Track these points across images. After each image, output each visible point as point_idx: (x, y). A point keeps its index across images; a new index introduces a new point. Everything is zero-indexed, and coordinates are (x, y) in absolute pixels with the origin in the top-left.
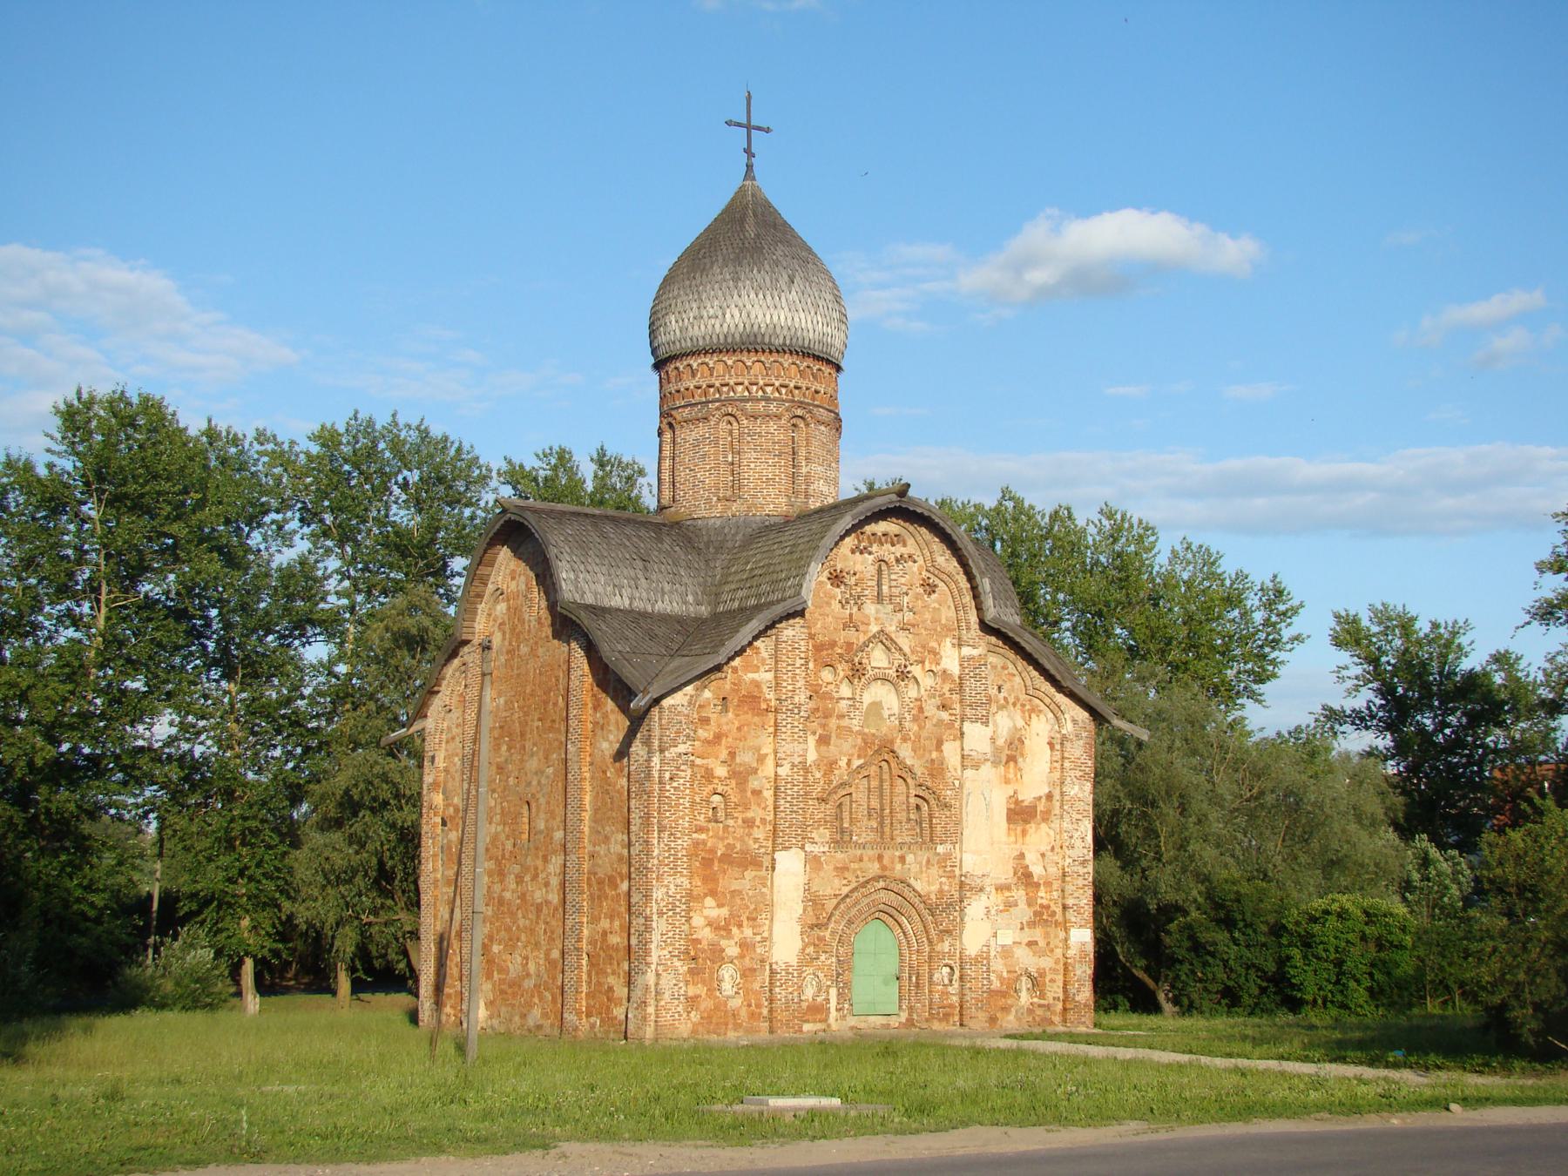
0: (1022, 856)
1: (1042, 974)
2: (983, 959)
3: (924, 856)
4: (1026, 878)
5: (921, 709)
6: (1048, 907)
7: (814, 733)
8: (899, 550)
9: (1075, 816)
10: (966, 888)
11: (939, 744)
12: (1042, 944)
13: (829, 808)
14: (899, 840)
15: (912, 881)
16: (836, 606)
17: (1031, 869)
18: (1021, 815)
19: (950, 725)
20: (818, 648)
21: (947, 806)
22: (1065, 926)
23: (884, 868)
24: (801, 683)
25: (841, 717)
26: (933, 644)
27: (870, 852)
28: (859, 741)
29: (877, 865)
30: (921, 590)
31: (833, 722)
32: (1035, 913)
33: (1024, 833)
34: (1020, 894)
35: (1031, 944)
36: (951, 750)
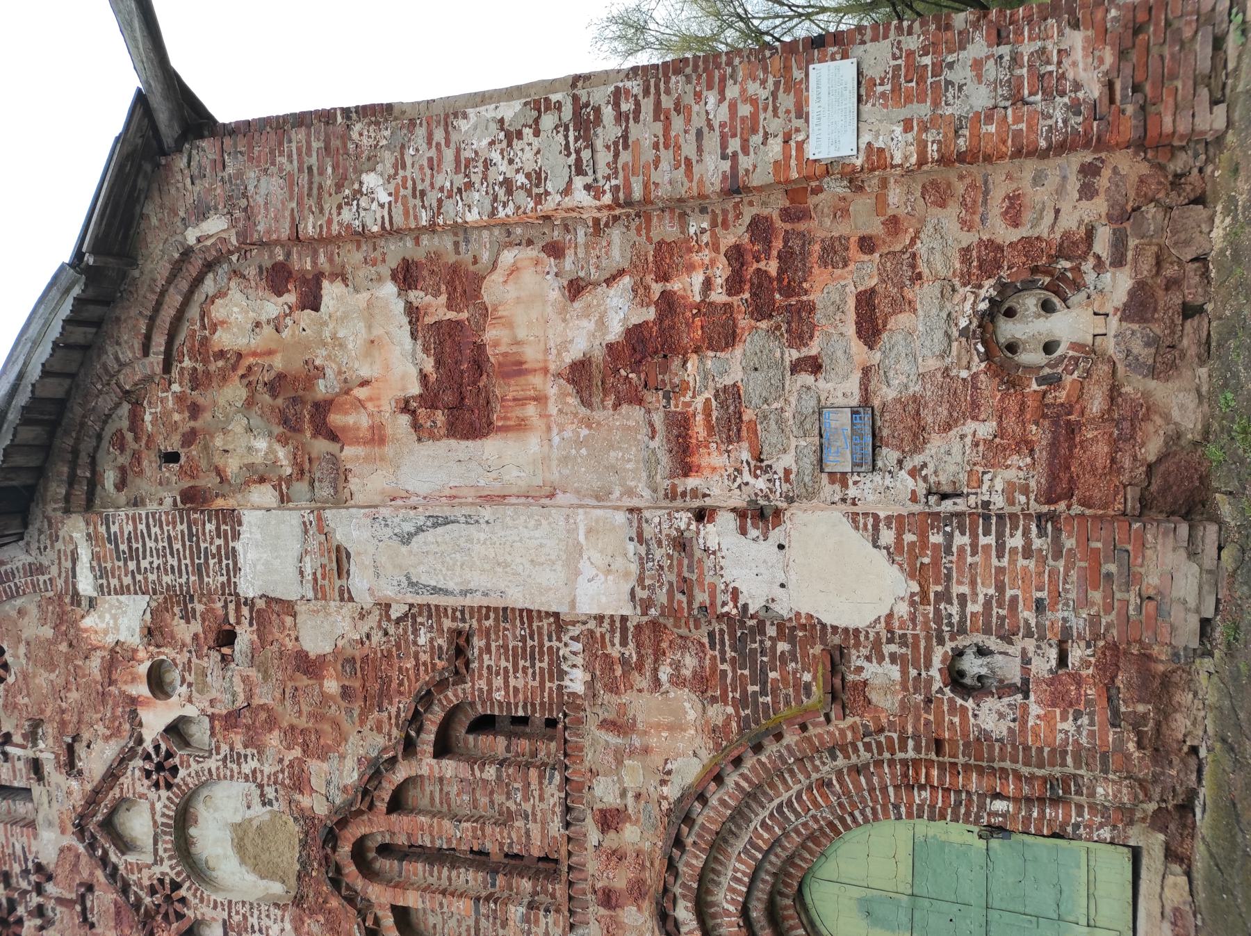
0: (579, 373)
1: (984, 260)
2: (924, 538)
3: (596, 743)
4: (640, 360)
5: (231, 720)
6: (736, 255)
9: (444, 180)
10: (681, 620)
11: (308, 666)
12: (864, 272)
15: (672, 792)
17: (615, 332)
18: (463, 392)
21: (460, 647)
22: (801, 187)
23: (637, 891)
26: (95, 665)
32: (761, 311)
33: (516, 368)
34: (701, 376)
35: (870, 328)
36: (320, 632)
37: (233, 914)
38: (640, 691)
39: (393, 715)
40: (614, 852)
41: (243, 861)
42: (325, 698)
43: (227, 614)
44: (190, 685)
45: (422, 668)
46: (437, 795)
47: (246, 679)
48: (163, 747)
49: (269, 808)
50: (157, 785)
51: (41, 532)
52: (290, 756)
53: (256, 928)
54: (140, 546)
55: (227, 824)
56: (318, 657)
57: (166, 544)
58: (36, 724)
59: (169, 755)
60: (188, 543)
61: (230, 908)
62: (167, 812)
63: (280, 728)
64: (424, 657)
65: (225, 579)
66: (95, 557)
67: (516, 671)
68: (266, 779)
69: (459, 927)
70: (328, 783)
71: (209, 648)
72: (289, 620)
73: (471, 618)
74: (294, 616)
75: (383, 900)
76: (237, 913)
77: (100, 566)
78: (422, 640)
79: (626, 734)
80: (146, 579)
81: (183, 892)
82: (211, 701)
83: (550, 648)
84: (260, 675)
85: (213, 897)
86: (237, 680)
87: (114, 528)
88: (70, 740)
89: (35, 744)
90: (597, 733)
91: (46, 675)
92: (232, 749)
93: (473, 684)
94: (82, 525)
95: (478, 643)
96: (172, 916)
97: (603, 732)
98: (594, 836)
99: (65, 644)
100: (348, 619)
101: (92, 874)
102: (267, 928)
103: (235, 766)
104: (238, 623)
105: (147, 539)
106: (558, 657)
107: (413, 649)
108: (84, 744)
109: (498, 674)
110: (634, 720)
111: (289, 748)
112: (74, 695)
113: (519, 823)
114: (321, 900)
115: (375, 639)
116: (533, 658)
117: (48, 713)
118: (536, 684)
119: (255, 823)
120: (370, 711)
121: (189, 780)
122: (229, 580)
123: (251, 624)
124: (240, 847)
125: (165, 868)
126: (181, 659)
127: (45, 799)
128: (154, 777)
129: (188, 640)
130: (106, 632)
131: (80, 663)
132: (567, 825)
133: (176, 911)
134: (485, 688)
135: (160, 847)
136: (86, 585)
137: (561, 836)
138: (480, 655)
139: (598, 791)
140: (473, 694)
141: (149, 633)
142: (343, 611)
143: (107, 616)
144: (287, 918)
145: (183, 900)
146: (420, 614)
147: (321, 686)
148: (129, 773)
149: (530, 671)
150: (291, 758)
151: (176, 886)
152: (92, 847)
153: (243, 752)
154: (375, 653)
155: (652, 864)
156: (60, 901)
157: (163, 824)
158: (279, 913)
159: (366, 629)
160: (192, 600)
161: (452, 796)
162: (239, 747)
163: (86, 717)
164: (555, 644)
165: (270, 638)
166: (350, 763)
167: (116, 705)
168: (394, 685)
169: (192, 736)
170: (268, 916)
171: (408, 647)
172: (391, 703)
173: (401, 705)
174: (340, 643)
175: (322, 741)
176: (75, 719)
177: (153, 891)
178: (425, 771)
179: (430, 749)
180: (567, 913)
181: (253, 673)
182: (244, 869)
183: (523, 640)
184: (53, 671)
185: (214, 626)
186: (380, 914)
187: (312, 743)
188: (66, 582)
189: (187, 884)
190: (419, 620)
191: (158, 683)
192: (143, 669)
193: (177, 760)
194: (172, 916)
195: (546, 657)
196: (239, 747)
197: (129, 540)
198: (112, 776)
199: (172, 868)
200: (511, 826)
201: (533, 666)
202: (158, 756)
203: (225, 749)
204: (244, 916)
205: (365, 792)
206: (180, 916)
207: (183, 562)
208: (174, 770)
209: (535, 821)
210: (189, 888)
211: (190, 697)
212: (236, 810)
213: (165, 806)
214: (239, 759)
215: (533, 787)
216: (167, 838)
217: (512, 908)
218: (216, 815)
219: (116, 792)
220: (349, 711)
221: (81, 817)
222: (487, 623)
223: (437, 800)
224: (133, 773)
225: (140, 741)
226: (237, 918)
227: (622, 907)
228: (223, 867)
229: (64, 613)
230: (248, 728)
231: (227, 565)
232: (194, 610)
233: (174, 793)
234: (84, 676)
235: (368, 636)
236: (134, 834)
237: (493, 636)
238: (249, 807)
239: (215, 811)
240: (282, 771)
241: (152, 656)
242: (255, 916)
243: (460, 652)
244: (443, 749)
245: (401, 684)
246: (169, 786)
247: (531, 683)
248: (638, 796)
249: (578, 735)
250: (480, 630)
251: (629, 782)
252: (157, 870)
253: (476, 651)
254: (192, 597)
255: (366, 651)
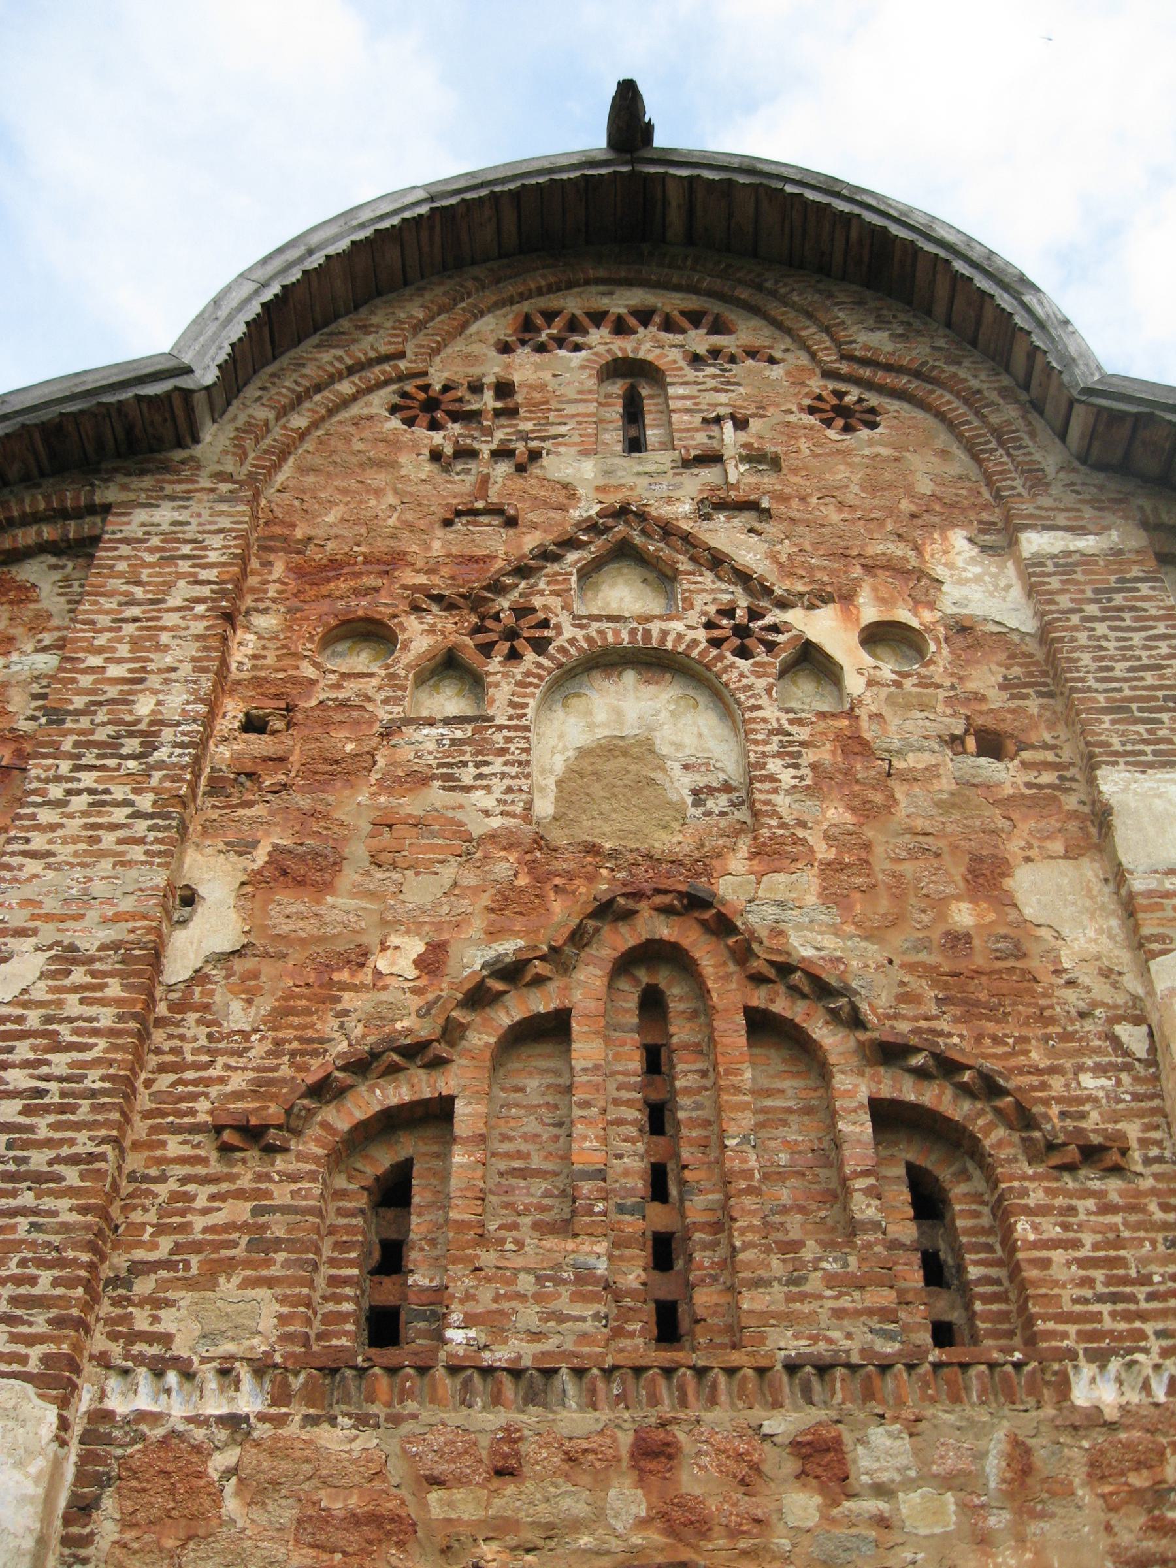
3: (984, 1435)
5: (854, 745)
7: (244, 848)
8: (699, 340)
11: (987, 876)
13: (296, 1180)
14: (786, 1343)
16: (415, 468)
19: (1040, 801)
20: (315, 574)
21: (1097, 1155)
24: (179, 653)
25: (419, 780)
27: (573, 1418)
28: (504, 866)
29: (627, 1502)
30: (812, 420)
31: (357, 804)
36: (1053, 896)
37: (505, 732)
38: (1109, 1528)
39: (933, 1024)
40: (756, 1468)
41: (583, 753)
42: (940, 904)
43: (1032, 747)
44: (898, 684)
45: (1035, 1080)
46: (778, 1103)
47: (932, 772)
48: (780, 638)
49: (689, 800)
50: (709, 625)
51: (1101, 488)
52: (813, 838)
53: (485, 770)
54: (1128, 623)
55: (651, 729)
56: (1009, 894)
57: (1145, 661)
58: (775, 463)
59: (770, 647)
60: (1160, 694)
61: (516, 728)
62: (670, 639)
63: (861, 825)
64: (1057, 1084)
65: (1117, 747)
66: (1087, 560)
67: (1083, 1263)
68: (763, 797)
69: (525, 1137)
70: (781, 904)
71: (968, 718)
72: (1058, 847)
73: (1156, 1176)
74: (1070, 855)
75: (578, 995)
76: (509, 740)
77: (1077, 564)
78: (1088, 1081)
79: (1010, 1495)
80: (1075, 628)
81: (530, 656)
82: (880, 716)
83: (1144, 1337)
84: (945, 796)
85: (532, 703)
86: (927, 759)
87: (1144, 589)
88: (765, 504)
89: (743, 459)
90: (1000, 1434)
91: (856, 478)
92: (802, 744)
93: (1032, 1179)
94: (1133, 544)
95: (1114, 1187)
96: (482, 638)
97: (1005, 1446)
98: (783, 1423)
99: (913, 508)
100: (1093, 948)
101: (534, 526)
102: (488, 788)
103: (774, 747)
104: (1025, 765)
105: (1143, 634)
106: (1130, 1351)
107: (1068, 1064)
108: (757, 525)
109: (1066, 1227)
110: (1042, 1516)
111: (827, 837)
112: (835, 516)
113: (777, 1266)
114: (557, 881)
115: (1070, 995)
116: (1114, 1298)
117: (793, 479)
118: (1067, 1306)
119: (658, 776)
120: (935, 984)
121: (734, 674)
122: (1116, 754)
123: (1029, 785)
124: (611, 749)
125: (569, 631)
126: (937, 672)
127: (650, 468)
128: (724, 622)
129: (972, 686)
130: (950, 565)
131: (889, 526)
132: (792, 1368)
133: (492, 644)
134: (1031, 1202)
135: (605, 625)
136: (1034, 542)
137: (770, 1355)
138: (1092, 1194)
139: (878, 1435)
140: (1012, 1178)
141: (962, 628)
142: (1104, 939)
143: (978, 570)
144: (510, 822)
145: (514, 655)
146: (1136, 1079)
147: (958, 898)
148: (724, 586)
149: (1088, 1293)
150: (811, 840)
151: (540, 646)
152: (592, 527)
153: (803, 762)
154: (1044, 995)
155: (744, 1553)
156: (485, 481)
157: (647, 632)
158: (519, 808)
159: (1085, 980)
160: (1040, 694)
161: (782, 1132)
162: (809, 756)
163: (801, 530)
164: (1155, 1345)
165: (1015, 816)
166: (829, 942)
167: (832, 572)
168: (991, 1027)
169: (794, 682)
170: (509, 790)
171: (1069, 1054)
172: (956, 1020)
173: (956, 1038)
174: (1043, 932)
175: (857, 896)
176: (792, 514)
177: (522, 611)
178: (842, 1081)
179: (886, 1091)
180: (609, 1362)
181: (946, 784)
182: (571, 754)
183: (1145, 1280)
184: (863, 489)
185: (1007, 727)
186: (551, 987)
187: (846, 877)
188: (1031, 516)
189: (546, 662)
190: (1125, 1077)
191: (876, 637)
192: (903, 615)
193: (764, 658)
194: (482, 638)
195: (1122, 1326)
196: (809, 756)
197: (1132, 609)
198: (716, 561)
199: (572, 641)
200: (768, 1250)
201: (1100, 1299)
202: (762, 629)
203: (803, 734)
204: (503, 752)
205: (785, 969)
206: (486, 649)
207: (1125, 686)
208: (743, 652)
209: (790, 1299)
210: (539, 666)
211: (877, 683)
212: (679, 746)
213: (680, 637)
214: (790, 754)
215: (857, 1295)
216: (625, 636)
217: (601, 1247)
218: (664, 715)
219: (684, 564)
220: (924, 945)
221: (642, 516)
222: (1153, 1207)
223: (768, 1103)
224: (726, 591)
225: (783, 605)
226: (499, 738)
227: (641, 1482)
228: (572, 720)
229: (963, 510)
230: (848, 772)
231: (1143, 753)
232: (1025, 697)
233: (705, 650)
234: (869, 531)
235: (1071, 983)
236: (605, 587)
237: (1133, 1218)
238: (686, 767)
239: (672, 713)
240: (783, 825)
241: (929, 630)
242: (507, 769)
243: (1091, 1154)
244: (888, 1117)
245: (996, 1040)
246: (716, 643)
247: (1067, 1294)
248: (883, 1522)
249: (983, 1392)
250: (1139, 1194)
251: (910, 1503)
252: (564, 619)
253: (1095, 1185)
254: (1050, 695)
255: (1047, 979)
